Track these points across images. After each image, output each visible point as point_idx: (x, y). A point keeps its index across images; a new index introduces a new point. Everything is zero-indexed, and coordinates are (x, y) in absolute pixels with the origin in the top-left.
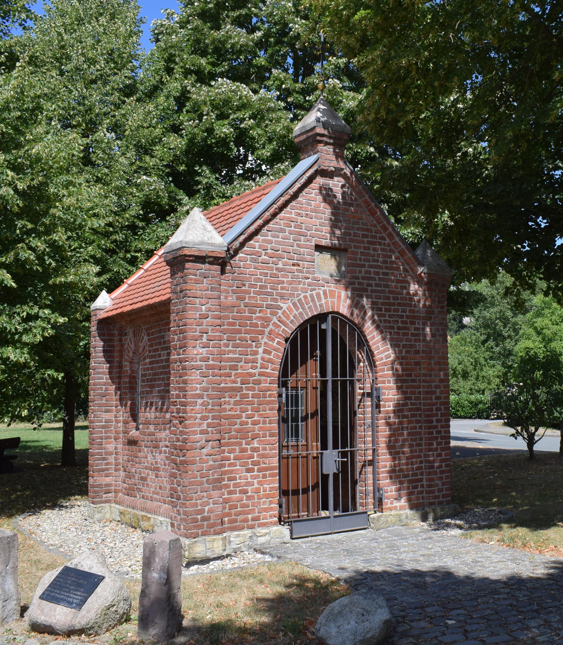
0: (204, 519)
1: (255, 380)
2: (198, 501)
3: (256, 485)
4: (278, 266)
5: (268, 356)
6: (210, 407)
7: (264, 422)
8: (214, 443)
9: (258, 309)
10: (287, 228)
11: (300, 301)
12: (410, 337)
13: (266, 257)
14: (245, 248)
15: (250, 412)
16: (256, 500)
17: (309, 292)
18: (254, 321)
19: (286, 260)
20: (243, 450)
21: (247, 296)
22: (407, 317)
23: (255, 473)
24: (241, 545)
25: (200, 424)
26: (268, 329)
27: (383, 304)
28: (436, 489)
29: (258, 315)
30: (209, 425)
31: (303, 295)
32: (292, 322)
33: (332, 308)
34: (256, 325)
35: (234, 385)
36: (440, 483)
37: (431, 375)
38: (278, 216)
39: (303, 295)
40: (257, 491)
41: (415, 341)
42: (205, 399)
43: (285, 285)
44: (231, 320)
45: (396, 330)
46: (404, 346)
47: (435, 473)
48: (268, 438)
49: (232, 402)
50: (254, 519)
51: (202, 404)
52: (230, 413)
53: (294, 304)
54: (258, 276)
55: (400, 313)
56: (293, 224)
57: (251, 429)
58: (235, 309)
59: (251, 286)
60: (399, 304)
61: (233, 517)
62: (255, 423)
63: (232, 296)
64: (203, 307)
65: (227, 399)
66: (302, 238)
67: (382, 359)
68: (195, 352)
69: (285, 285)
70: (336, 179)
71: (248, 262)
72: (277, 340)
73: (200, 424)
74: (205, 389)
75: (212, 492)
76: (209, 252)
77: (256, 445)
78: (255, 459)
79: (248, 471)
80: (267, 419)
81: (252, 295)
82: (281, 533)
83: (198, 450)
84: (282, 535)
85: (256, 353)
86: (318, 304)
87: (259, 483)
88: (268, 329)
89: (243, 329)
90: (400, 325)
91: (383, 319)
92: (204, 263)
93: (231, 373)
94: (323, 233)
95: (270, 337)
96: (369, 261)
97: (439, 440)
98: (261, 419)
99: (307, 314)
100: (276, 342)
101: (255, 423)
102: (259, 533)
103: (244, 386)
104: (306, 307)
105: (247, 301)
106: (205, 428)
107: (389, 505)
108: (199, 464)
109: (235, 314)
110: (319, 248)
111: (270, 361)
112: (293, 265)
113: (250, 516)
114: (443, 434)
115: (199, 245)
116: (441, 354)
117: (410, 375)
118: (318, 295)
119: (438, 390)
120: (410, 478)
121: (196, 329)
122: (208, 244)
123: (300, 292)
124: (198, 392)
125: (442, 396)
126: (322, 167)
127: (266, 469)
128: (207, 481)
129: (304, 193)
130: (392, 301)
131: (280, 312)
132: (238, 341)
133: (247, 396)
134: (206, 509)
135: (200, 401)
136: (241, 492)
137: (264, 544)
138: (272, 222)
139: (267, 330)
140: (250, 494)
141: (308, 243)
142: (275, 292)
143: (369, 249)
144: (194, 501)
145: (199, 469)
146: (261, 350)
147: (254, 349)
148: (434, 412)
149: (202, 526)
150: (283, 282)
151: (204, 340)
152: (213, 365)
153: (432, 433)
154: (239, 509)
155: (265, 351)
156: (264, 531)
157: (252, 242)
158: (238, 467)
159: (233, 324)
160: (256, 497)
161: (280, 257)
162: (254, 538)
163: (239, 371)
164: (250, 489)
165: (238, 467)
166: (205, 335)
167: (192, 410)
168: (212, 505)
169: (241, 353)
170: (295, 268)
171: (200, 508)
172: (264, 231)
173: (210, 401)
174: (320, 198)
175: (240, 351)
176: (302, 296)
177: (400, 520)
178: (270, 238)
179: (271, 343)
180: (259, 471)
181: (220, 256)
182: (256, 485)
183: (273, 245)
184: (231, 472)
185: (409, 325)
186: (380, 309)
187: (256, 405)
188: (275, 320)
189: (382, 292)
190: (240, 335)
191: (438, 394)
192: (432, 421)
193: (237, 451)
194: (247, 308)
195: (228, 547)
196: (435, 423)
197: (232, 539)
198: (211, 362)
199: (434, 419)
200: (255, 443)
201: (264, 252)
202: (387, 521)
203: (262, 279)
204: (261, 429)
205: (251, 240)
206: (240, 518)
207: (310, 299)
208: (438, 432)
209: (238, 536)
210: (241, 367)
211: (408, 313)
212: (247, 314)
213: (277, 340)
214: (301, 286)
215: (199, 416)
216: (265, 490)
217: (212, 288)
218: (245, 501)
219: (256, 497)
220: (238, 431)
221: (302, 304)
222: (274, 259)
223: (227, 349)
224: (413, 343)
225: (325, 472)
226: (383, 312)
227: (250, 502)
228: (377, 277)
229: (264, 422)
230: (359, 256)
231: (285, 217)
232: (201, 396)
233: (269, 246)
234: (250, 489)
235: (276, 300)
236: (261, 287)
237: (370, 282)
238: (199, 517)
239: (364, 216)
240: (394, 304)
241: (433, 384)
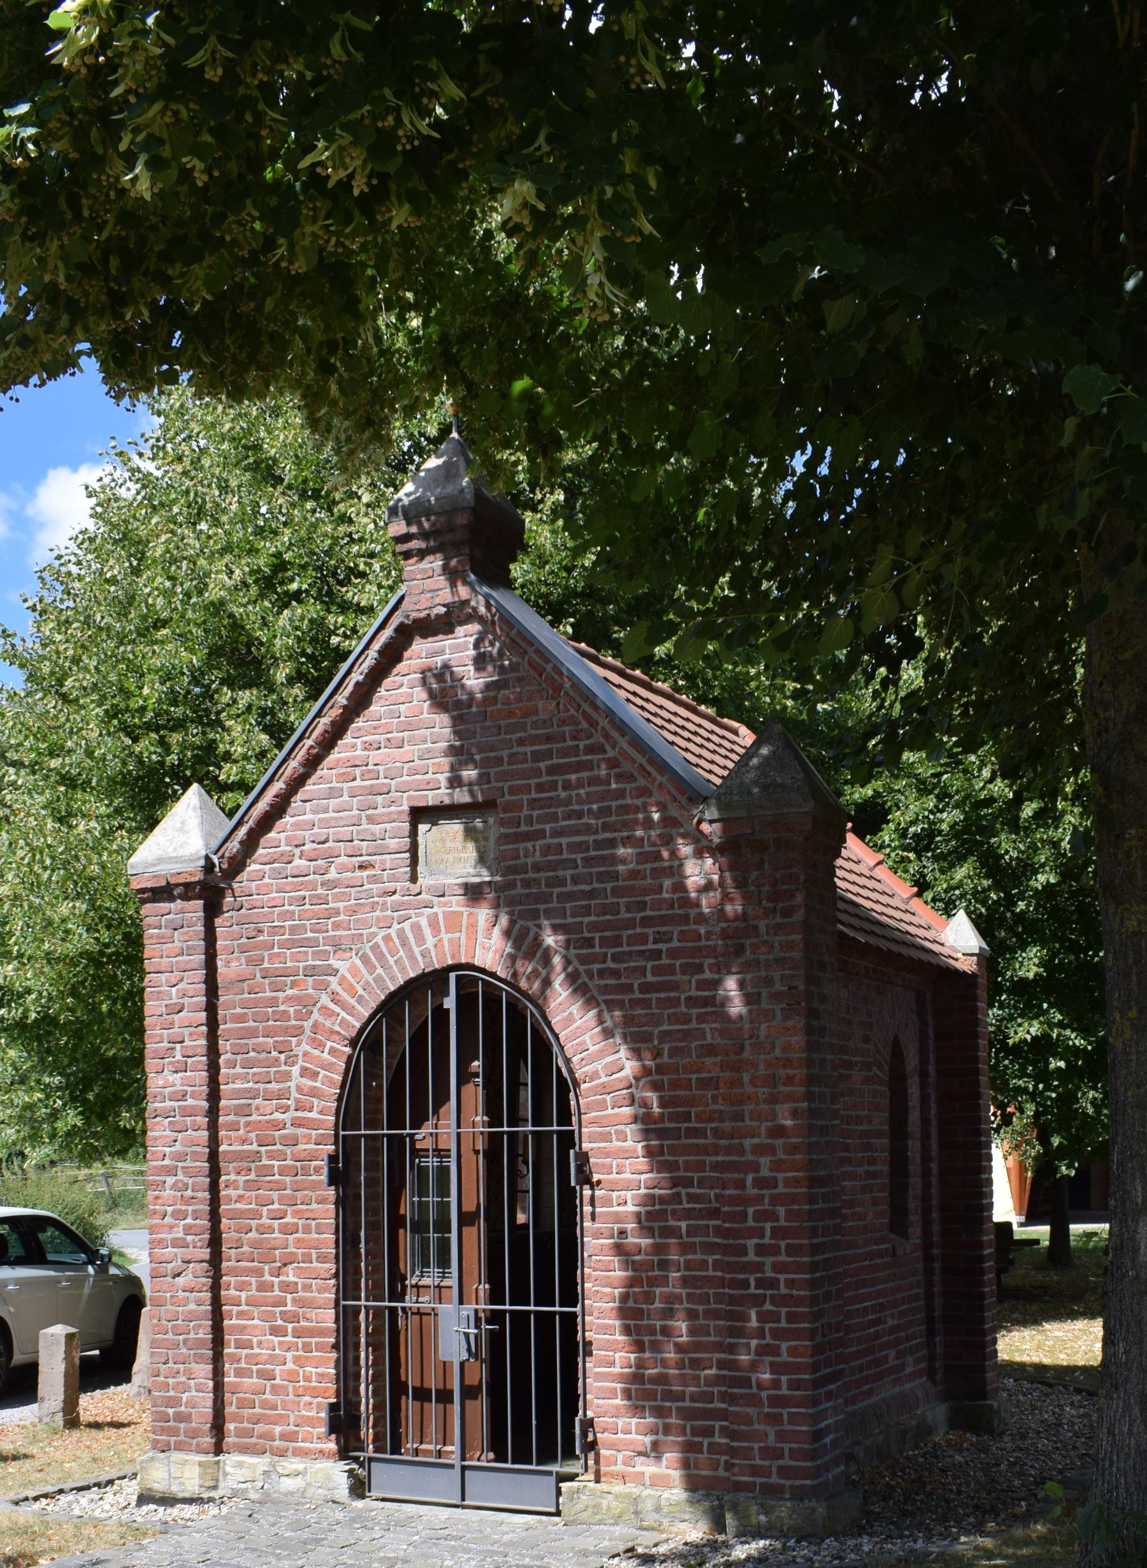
0: (180, 1418)
1: (283, 1137)
2: (170, 1381)
3: (290, 1365)
4: (326, 877)
5: (310, 1083)
6: (189, 1193)
7: (307, 1229)
8: (198, 1266)
9: (289, 980)
10: (346, 785)
11: (375, 947)
12: (683, 1009)
13: (303, 862)
14: (260, 851)
15: (276, 1206)
16: (291, 1396)
17: (396, 926)
18: (282, 1008)
19: (343, 859)
20: (264, 1287)
21: (266, 954)
22: (673, 953)
23: (289, 1338)
24: (248, 1485)
25: (171, 1227)
26: (310, 1022)
27: (594, 927)
28: (756, 1446)
29: (290, 992)
30: (188, 1230)
31: (383, 933)
32: (360, 1000)
33: (453, 957)
34: (285, 1016)
35: (246, 1147)
36: (771, 1431)
37: (739, 1117)
38: (325, 763)
39: (383, 933)
40: (292, 1377)
41: (701, 1018)
42: (180, 1176)
43: (342, 917)
44: (238, 1010)
45: (637, 995)
46: (665, 1036)
47: (753, 1400)
48: (315, 1264)
49: (241, 1184)
50: (284, 1437)
51: (174, 1187)
52: (238, 1205)
53: (365, 959)
54: (287, 907)
55: (651, 946)
56: (358, 771)
57: (278, 1243)
58: (245, 984)
59: (275, 931)
60: (646, 922)
61: (245, 1425)
62: (287, 1230)
63: (238, 959)
64: (174, 990)
65: (233, 1177)
66: (379, 799)
67: (595, 1076)
68: (161, 1082)
69: (342, 917)
70: (460, 630)
71: (266, 880)
72: (329, 1044)
73: (171, 1227)
74: (180, 1157)
75: (193, 1365)
76: (173, 875)
77: (292, 1278)
78: (289, 1308)
79: (276, 1331)
80: (313, 1223)
81: (276, 950)
82: (329, 1478)
83: (169, 1279)
84: (331, 1485)
85: (287, 1076)
86: (417, 951)
87: (296, 1360)
88: (310, 1022)
89: (261, 1025)
90: (650, 978)
91: (596, 967)
92: (172, 899)
93: (238, 1123)
94: (429, 776)
95: (314, 1040)
96: (554, 818)
97: (768, 1306)
98: (301, 1222)
99: (393, 979)
100: (327, 1050)
101: (287, 1230)
102: (284, 1468)
103: (263, 1149)
104: (391, 961)
105: (266, 965)
106: (181, 1235)
107: (619, 1467)
108: (169, 1307)
109: (246, 995)
110: (419, 815)
111: (314, 1093)
112: (361, 867)
113: (278, 1429)
114: (783, 1290)
115: (154, 865)
116: (778, 1052)
117: (687, 1117)
118: (416, 928)
119: (765, 1161)
120: (687, 1404)
121: (161, 1035)
122: (171, 860)
123: (374, 929)
124: (167, 1162)
125: (781, 1176)
126: (414, 615)
127: (311, 1333)
128: (185, 1341)
129: (382, 692)
130: (624, 915)
131: (333, 981)
132: (252, 1054)
133: (267, 1171)
134: (185, 1396)
135: (170, 1180)
136: (262, 1374)
137: (292, 1493)
138: (310, 781)
139: (307, 1025)
140: (278, 1381)
141: (393, 809)
142: (320, 936)
143: (553, 786)
144: (161, 1379)
145: (169, 1317)
146: (295, 1070)
147: (284, 1068)
148: (751, 1223)
149: (175, 1432)
150: (337, 912)
151: (178, 1057)
152: (192, 1107)
153: (745, 1284)
154: (257, 1410)
155: (304, 1072)
156: (294, 1464)
157: (272, 835)
158: (256, 1322)
159: (241, 1018)
160: (291, 1389)
161: (331, 856)
162: (274, 1476)
163: (254, 1117)
164: (278, 1370)
165: (256, 1322)
166: (178, 1046)
167: (157, 1198)
168: (194, 1393)
169: (257, 1078)
170: (365, 873)
171: (172, 1393)
172: (296, 803)
173: (190, 1181)
174: (420, 693)
175: (255, 1074)
176: (378, 939)
177: (636, 1513)
178: (309, 817)
179: (316, 1052)
180: (297, 1334)
181: (193, 879)
182: (290, 1365)
183: (316, 830)
184: (243, 1329)
185: (678, 977)
186: (589, 943)
187: (288, 1192)
188: (325, 1000)
189: (592, 895)
190: (254, 1040)
191: (765, 1172)
192: (743, 1251)
193: (254, 1286)
194: (267, 981)
195: (222, 1484)
196: (752, 1257)
197: (228, 1469)
198: (190, 1102)
199: (751, 1243)
200: (291, 1273)
201: (297, 851)
202: (597, 1506)
203: (293, 912)
204: (299, 1243)
205: (269, 830)
206: (260, 1428)
207: (397, 941)
208: (773, 1284)
209: (240, 1465)
210: (257, 1109)
211: (675, 944)
212: (268, 994)
213: (329, 1044)
214: (378, 913)
215: (170, 1209)
216: (308, 1379)
217: (188, 948)
218: (268, 1396)
219: (291, 1389)
220: (255, 1245)
221: (381, 956)
222: (320, 862)
223: (232, 1071)
224: (694, 1025)
225: (442, 1357)
226: (597, 949)
227: (278, 1399)
228: (579, 857)
229: (307, 1229)
230: (526, 812)
231: (338, 760)
232: (171, 1171)
233: (307, 834)
234: (278, 1370)
235: (324, 955)
236: (293, 930)
237: (560, 873)
238: (171, 1411)
239: (540, 704)
240: (630, 924)
241: (748, 1143)
